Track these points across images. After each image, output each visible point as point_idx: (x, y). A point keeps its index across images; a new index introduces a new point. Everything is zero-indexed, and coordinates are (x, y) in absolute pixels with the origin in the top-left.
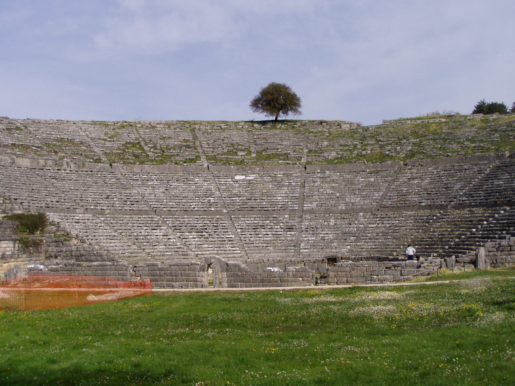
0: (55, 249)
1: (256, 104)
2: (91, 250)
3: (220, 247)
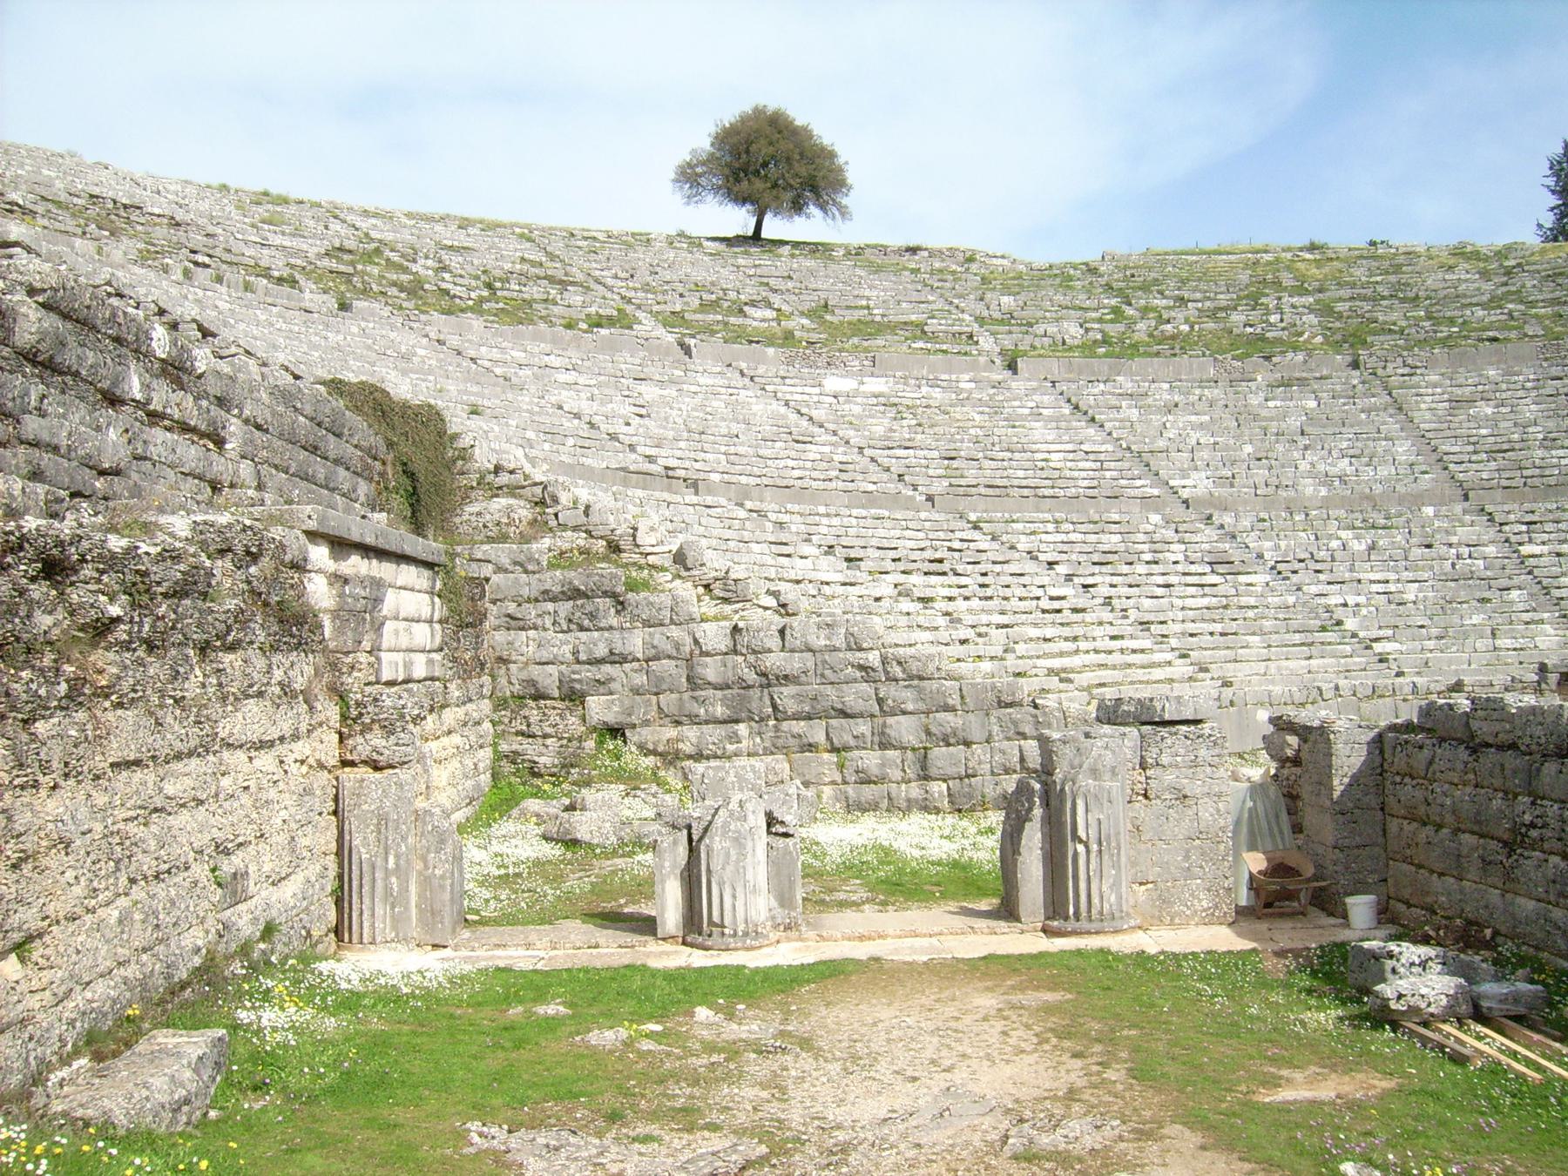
0: (562, 645)
1: (690, 177)
2: (839, 641)
3: (1075, 639)
